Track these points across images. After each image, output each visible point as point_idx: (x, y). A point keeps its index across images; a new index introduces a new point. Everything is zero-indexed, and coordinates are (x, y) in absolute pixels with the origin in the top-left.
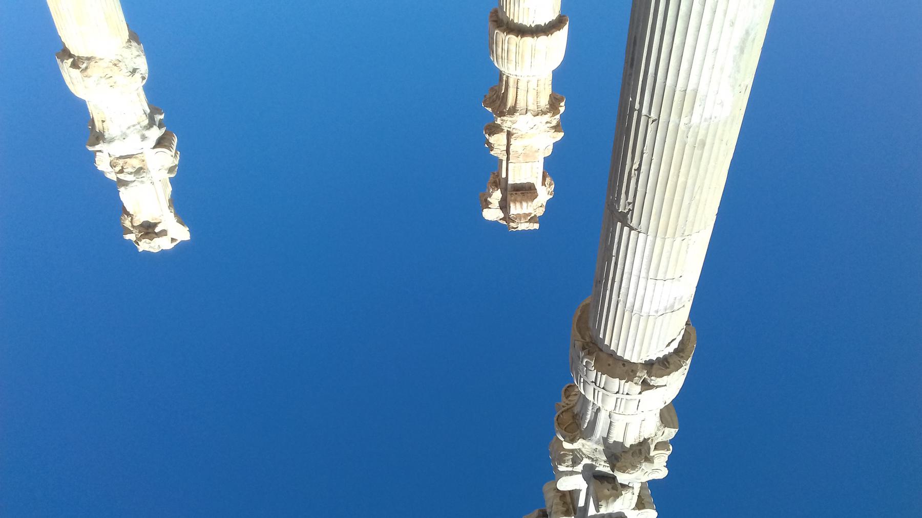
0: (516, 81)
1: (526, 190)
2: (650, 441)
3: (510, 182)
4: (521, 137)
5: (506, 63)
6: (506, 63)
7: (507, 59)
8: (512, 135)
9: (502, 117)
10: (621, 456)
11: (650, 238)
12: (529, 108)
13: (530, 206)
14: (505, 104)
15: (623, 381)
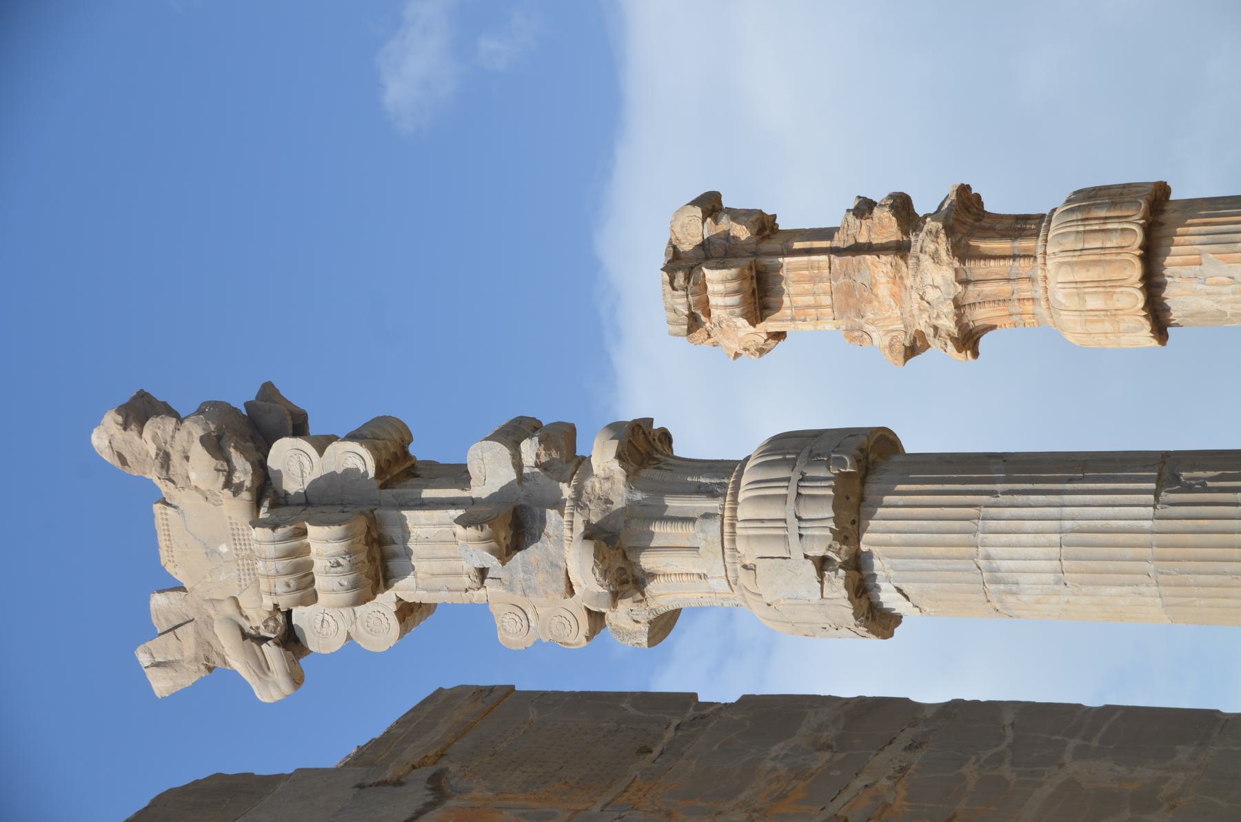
0: (1032, 254)
1: (760, 298)
2: (639, 597)
3: (787, 261)
4: (897, 278)
5: (1074, 229)
6: (1074, 229)
7: (1085, 232)
8: (902, 257)
9: (943, 231)
10: (617, 549)
11: (1147, 524)
12: (971, 287)
13: (732, 314)
14: (971, 235)
15: (832, 524)
